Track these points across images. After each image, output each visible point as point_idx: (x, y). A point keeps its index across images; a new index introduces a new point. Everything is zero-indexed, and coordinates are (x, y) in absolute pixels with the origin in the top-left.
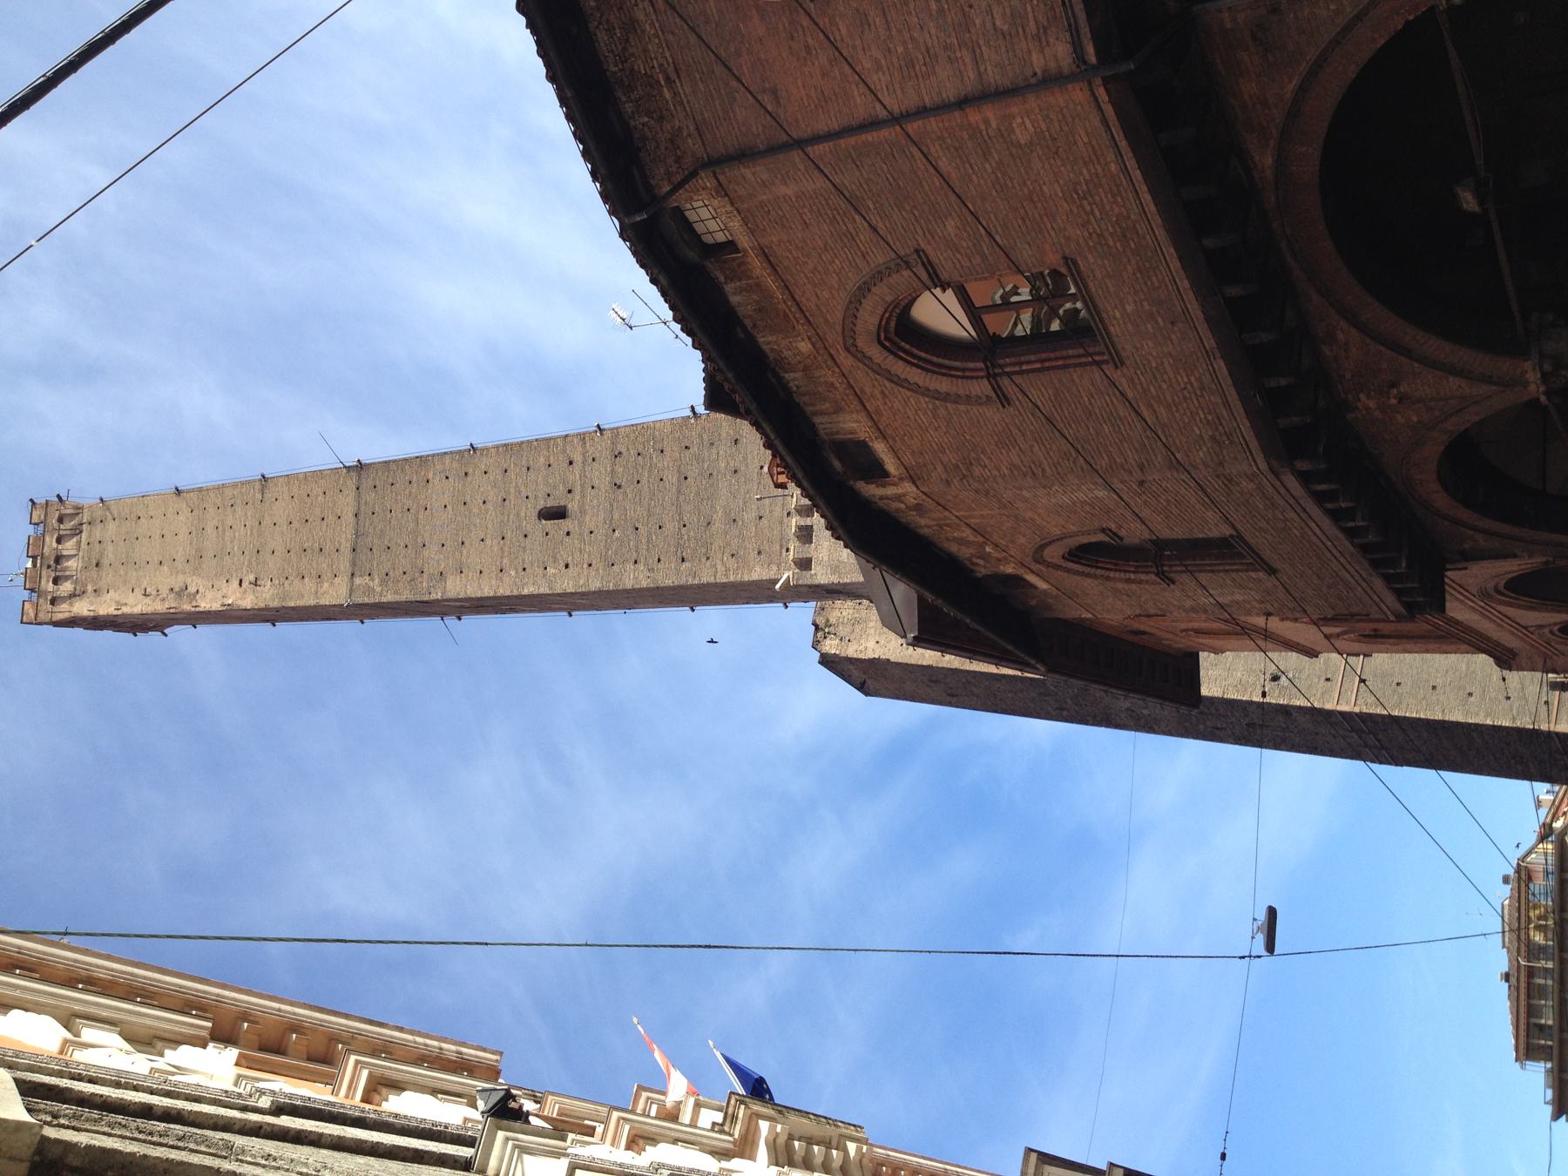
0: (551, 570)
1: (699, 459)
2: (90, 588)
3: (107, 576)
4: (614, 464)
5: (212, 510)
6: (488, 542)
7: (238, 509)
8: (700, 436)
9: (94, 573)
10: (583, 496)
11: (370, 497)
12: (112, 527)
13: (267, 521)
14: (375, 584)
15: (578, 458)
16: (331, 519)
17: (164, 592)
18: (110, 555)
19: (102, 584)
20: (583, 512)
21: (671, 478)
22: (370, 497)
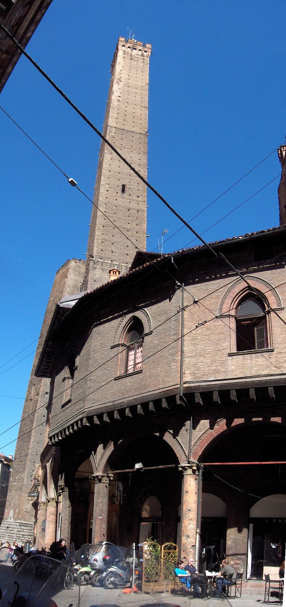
0: (107, 186)
1: (133, 236)
2: (125, 56)
3: (128, 61)
4: (135, 210)
5: (141, 92)
6: (119, 168)
7: (141, 99)
8: (140, 237)
9: (130, 58)
10: (128, 199)
11: (138, 136)
12: (142, 64)
13: (136, 107)
14: (112, 134)
15: (139, 199)
16: (133, 124)
17: (120, 75)
18: (133, 62)
19: (126, 59)
20: (124, 198)
21: (129, 227)
22: (138, 136)
